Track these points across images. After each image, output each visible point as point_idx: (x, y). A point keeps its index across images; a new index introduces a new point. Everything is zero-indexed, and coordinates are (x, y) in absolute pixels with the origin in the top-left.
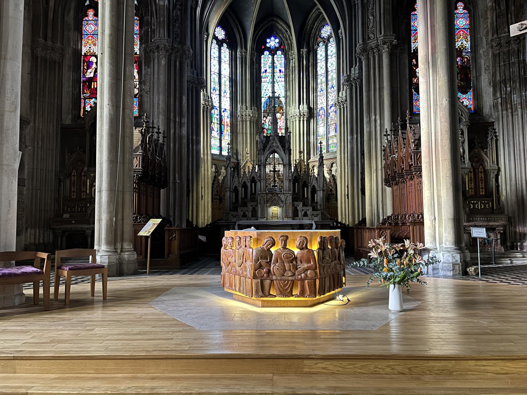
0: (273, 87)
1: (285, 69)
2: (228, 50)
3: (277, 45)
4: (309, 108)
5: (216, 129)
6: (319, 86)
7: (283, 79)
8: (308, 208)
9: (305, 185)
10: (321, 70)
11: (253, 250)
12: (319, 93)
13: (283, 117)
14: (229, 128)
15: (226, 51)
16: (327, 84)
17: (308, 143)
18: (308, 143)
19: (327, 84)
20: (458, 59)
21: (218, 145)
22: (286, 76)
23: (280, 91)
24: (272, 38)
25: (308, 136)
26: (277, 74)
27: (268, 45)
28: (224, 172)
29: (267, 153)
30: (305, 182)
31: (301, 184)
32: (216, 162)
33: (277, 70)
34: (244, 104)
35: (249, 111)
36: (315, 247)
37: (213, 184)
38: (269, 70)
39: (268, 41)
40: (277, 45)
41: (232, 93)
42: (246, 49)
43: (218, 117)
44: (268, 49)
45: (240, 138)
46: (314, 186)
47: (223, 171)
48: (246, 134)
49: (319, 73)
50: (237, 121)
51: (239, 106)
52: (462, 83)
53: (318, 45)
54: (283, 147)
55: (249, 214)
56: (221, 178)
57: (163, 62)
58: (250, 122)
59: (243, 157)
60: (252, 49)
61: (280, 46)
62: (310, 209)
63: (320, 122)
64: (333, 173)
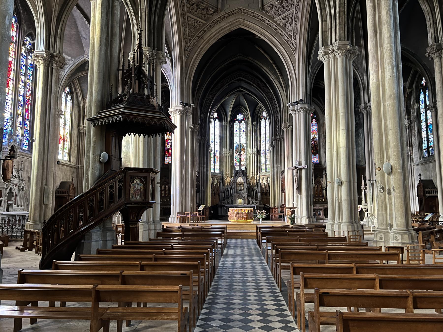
0: (240, 138)
1: (246, 130)
2: (218, 122)
4: (257, 150)
5: (212, 160)
6: (262, 139)
7: (245, 135)
8: (254, 200)
9: (253, 190)
10: (263, 132)
11: (235, 212)
12: (262, 143)
13: (245, 153)
14: (219, 159)
15: (217, 122)
16: (266, 139)
17: (257, 167)
18: (257, 167)
19: (266, 139)
21: (214, 168)
22: (246, 133)
23: (243, 141)
24: (240, 115)
26: (242, 132)
27: (237, 118)
29: (237, 177)
30: (253, 189)
31: (251, 190)
32: (212, 176)
33: (242, 130)
35: (228, 152)
36: (247, 212)
37: (211, 187)
38: (238, 130)
39: (237, 116)
40: (242, 118)
41: (220, 142)
42: (227, 122)
43: (214, 154)
44: (238, 120)
45: (224, 164)
46: (256, 191)
47: (216, 180)
48: (227, 162)
49: (262, 133)
50: (222, 156)
51: (223, 149)
53: (262, 120)
54: (244, 175)
55: (230, 202)
56: (215, 184)
57: (198, 145)
58: (229, 156)
59: (225, 173)
60: (230, 122)
61: (243, 119)
62: (255, 200)
63: (262, 157)
64: (268, 182)
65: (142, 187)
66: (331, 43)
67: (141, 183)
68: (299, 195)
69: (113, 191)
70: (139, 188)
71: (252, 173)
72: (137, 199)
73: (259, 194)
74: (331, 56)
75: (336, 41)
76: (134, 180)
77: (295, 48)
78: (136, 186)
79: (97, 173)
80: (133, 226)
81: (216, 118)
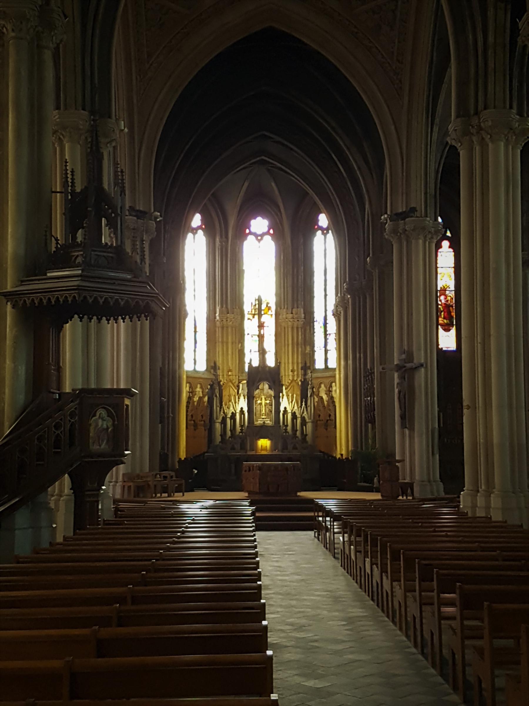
3: (266, 229)
20: (442, 298)
25: (303, 346)
27: (253, 229)
28: (199, 391)
32: (190, 380)
34: (224, 306)
37: (187, 407)
47: (198, 389)
52: (445, 321)
56: (196, 399)
59: (223, 372)
65: (110, 424)
66: (477, 113)
67: (108, 416)
68: (407, 431)
69: (61, 432)
70: (105, 426)
71: (293, 371)
72: (102, 447)
73: (309, 426)
74: (474, 139)
75: (485, 108)
76: (96, 412)
77: (400, 81)
78: (100, 422)
79: (21, 398)
80: (92, 499)
81: (199, 228)
